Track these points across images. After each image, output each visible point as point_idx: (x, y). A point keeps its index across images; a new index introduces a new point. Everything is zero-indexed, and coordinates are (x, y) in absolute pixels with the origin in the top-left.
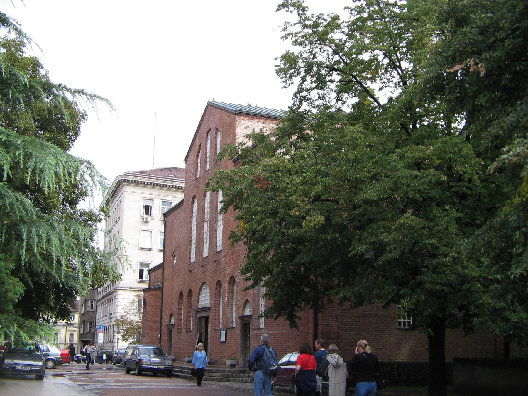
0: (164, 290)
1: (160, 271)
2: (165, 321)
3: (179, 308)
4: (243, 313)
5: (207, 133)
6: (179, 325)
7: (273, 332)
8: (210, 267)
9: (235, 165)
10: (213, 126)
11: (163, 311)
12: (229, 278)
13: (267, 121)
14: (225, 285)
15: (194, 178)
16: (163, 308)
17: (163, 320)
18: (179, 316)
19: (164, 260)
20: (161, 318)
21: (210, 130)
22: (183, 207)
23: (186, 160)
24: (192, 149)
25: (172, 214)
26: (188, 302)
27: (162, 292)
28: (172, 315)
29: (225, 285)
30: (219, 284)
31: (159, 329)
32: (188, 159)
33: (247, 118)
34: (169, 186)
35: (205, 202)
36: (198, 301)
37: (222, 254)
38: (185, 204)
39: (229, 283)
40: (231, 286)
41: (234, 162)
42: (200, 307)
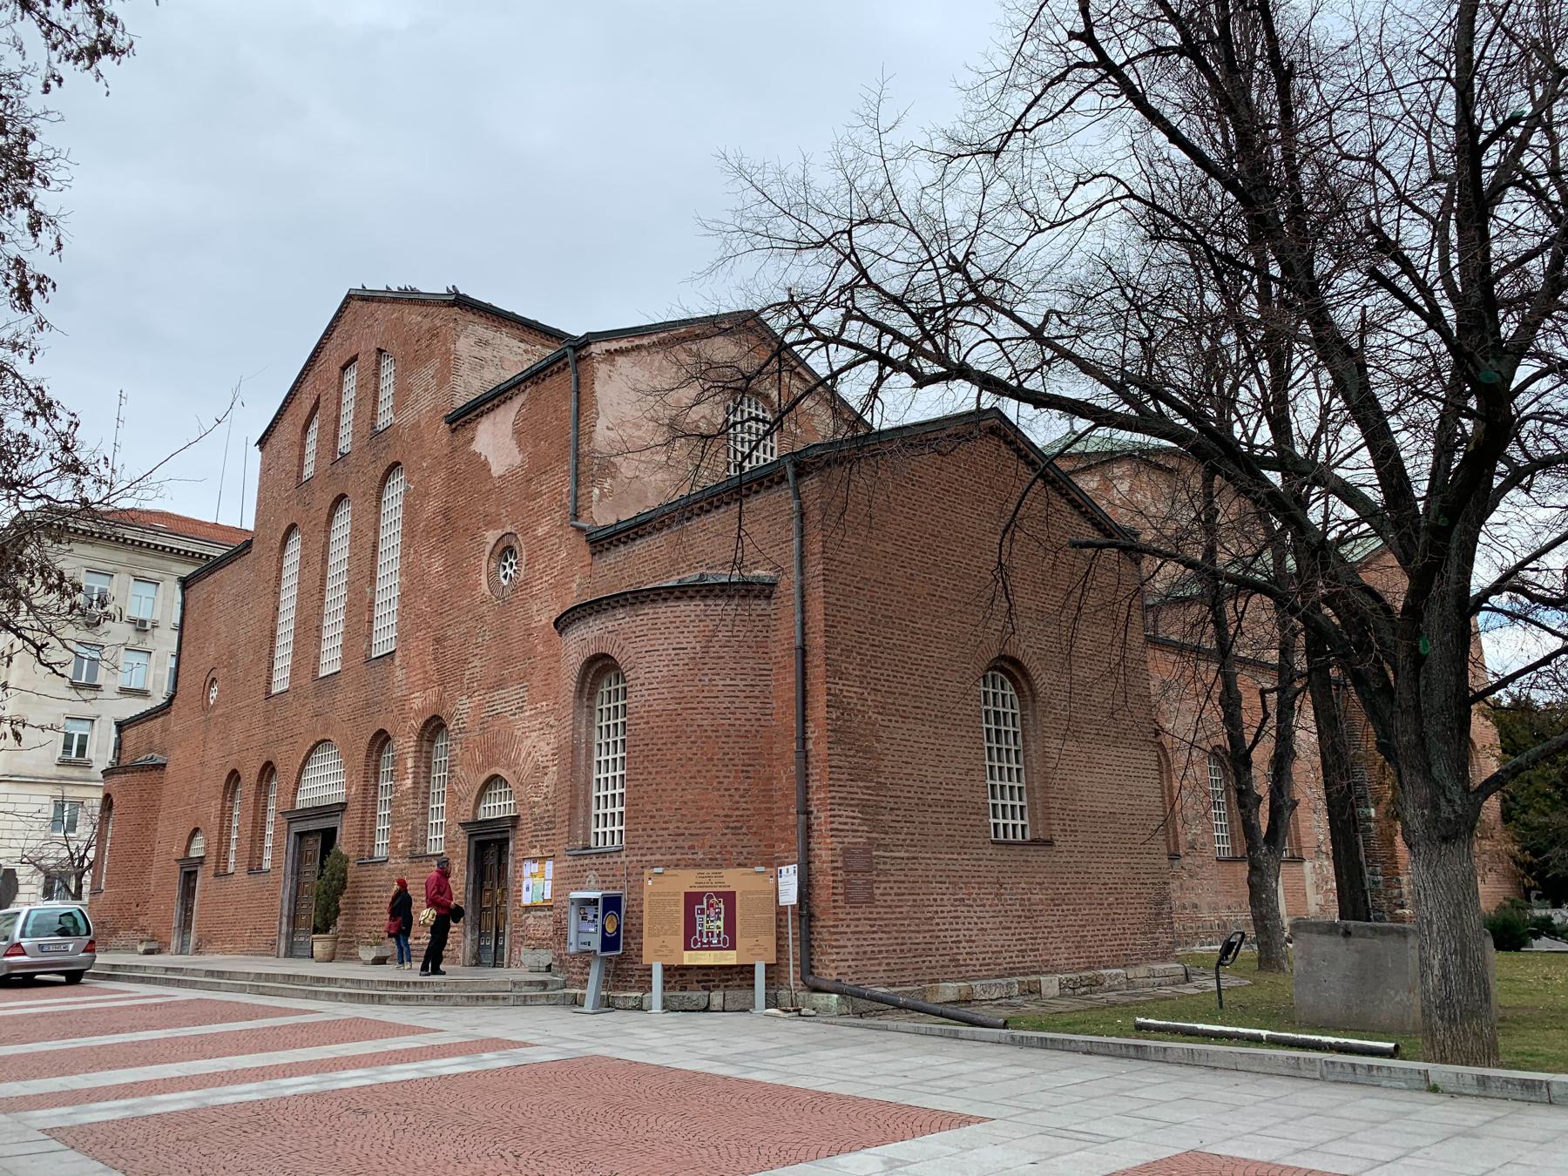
3: (225, 815)
4: (475, 814)
5: (344, 368)
6: (222, 857)
7: (658, 857)
8: (346, 699)
9: (454, 431)
10: (366, 348)
12: (421, 721)
13: (531, 337)
14: (405, 744)
15: (292, 483)
18: (221, 833)
21: (354, 359)
23: (262, 442)
24: (287, 414)
25: (211, 579)
26: (257, 795)
29: (405, 744)
30: (381, 739)
32: (272, 440)
37: (397, 662)
38: (255, 548)
39: (421, 737)
41: (450, 423)
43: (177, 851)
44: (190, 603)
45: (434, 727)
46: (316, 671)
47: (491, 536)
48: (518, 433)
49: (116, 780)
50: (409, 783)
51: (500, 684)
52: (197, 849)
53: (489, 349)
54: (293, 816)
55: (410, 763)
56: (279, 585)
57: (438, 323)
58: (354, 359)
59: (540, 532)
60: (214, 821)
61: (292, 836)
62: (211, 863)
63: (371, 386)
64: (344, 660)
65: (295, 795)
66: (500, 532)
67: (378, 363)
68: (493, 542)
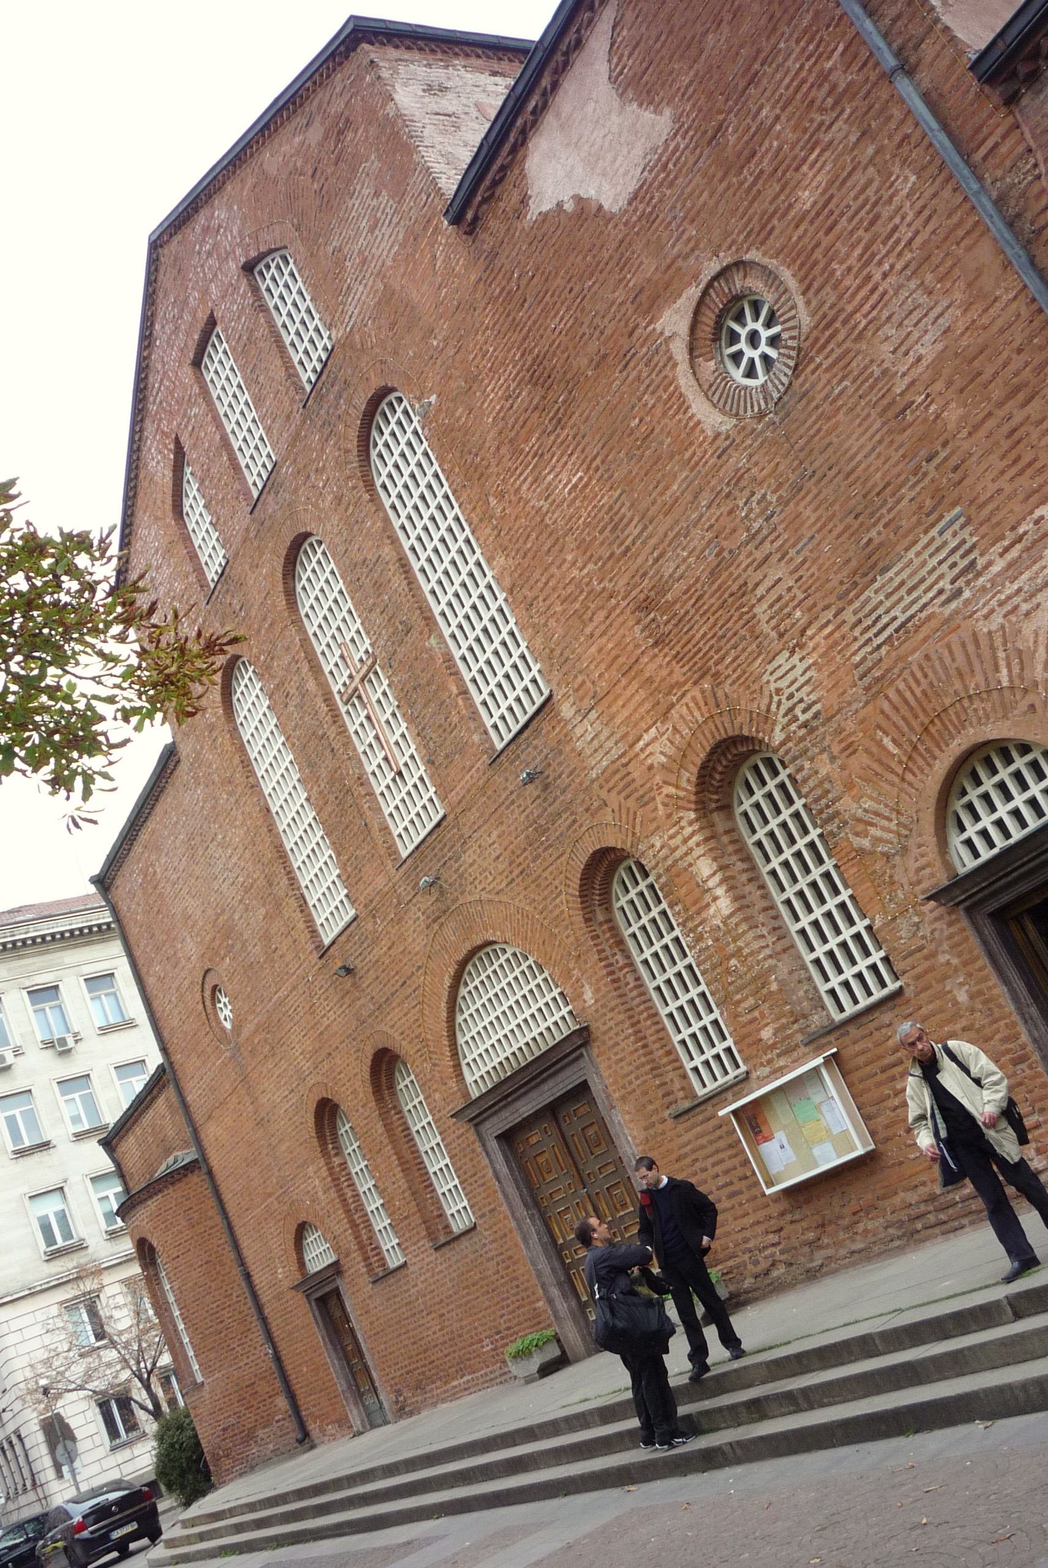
0: (215, 1161)
1: (170, 1092)
2: (275, 1276)
4: (948, 865)
5: (197, 363)
6: (369, 1249)
11: (244, 1242)
12: (688, 777)
14: (677, 840)
16: (239, 1231)
17: (260, 1279)
18: (347, 1211)
19: (164, 1050)
20: (248, 1276)
22: (184, 766)
25: (138, 848)
26: (384, 1116)
27: (210, 1173)
28: (301, 1231)
31: (256, 1324)
33: (416, 55)
34: (34, 939)
35: (302, 630)
36: (457, 1066)
37: (567, 710)
38: (184, 750)
39: (702, 809)
40: (716, 817)
42: (475, 1093)
43: (284, 1274)
44: (123, 907)
45: (727, 766)
46: (392, 851)
47: (674, 321)
48: (638, 85)
49: (143, 1215)
50: (724, 904)
51: (871, 564)
52: (319, 1255)
53: (450, 95)
54: (476, 1112)
55: (705, 868)
56: (252, 773)
57: (337, 106)
58: (212, 322)
59: (806, 198)
60: (326, 1198)
61: (493, 1145)
62: (355, 1266)
63: (262, 331)
64: (443, 792)
65: (460, 1075)
66: (693, 292)
67: (255, 290)
68: (683, 327)
